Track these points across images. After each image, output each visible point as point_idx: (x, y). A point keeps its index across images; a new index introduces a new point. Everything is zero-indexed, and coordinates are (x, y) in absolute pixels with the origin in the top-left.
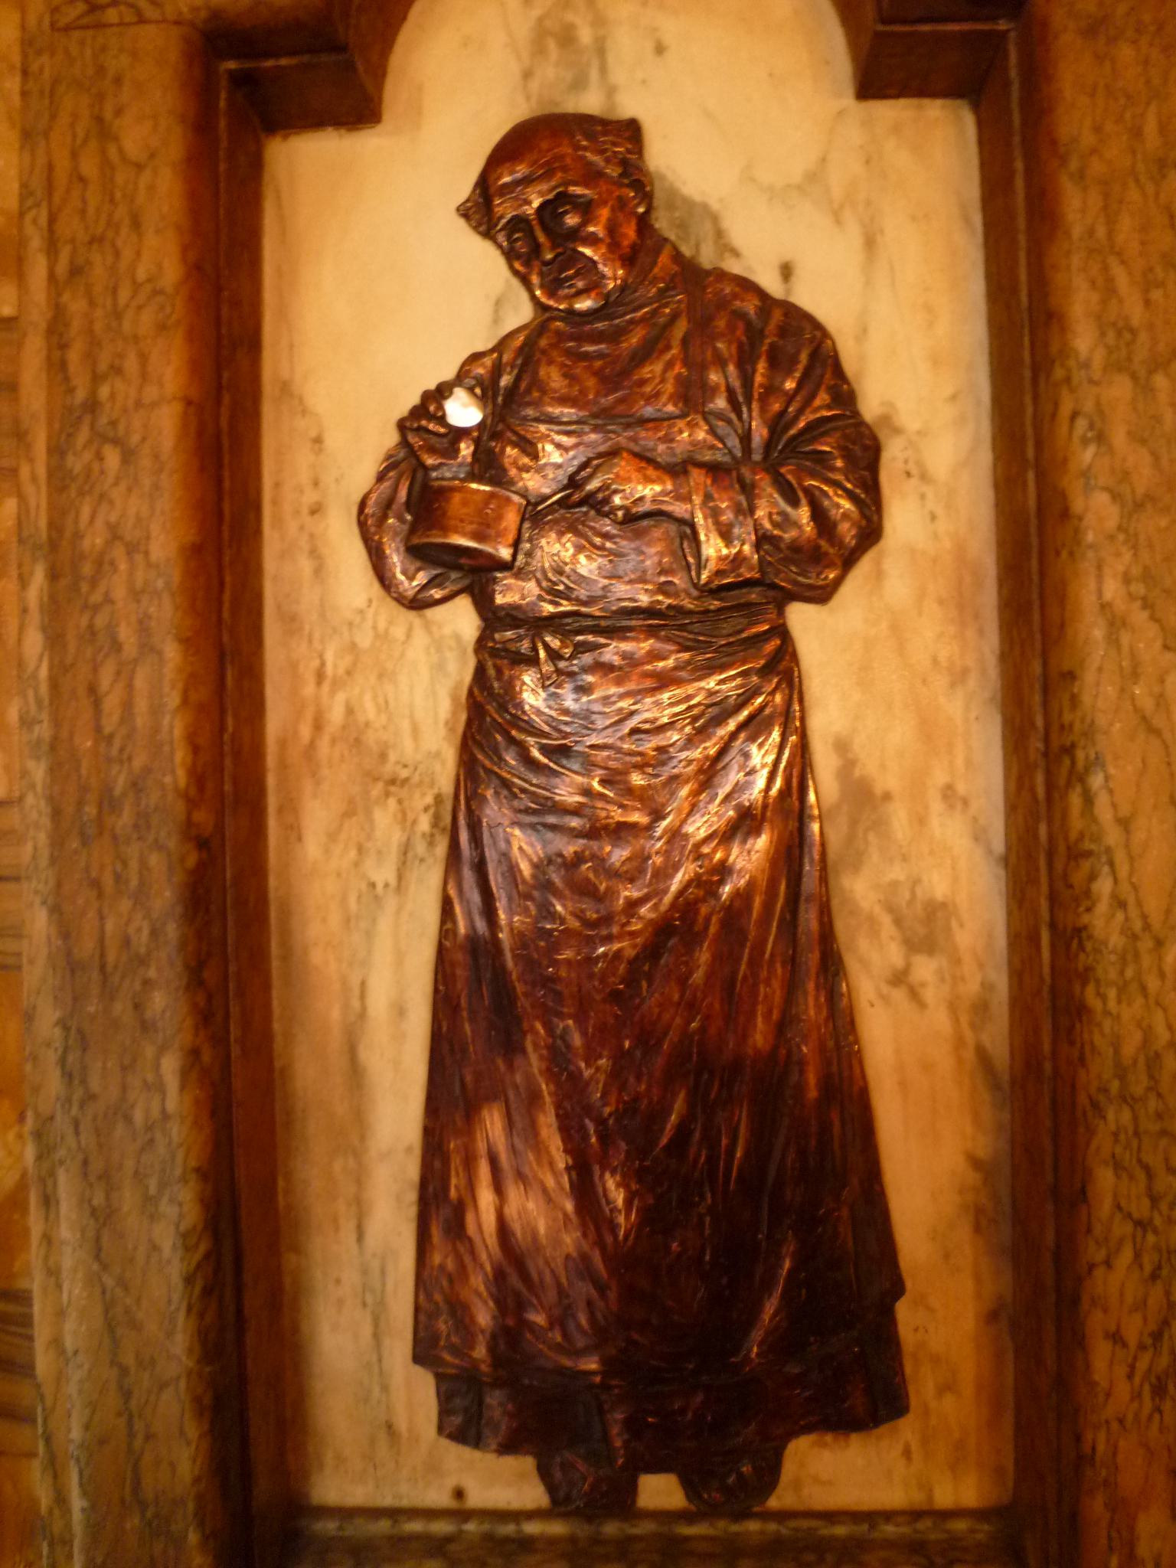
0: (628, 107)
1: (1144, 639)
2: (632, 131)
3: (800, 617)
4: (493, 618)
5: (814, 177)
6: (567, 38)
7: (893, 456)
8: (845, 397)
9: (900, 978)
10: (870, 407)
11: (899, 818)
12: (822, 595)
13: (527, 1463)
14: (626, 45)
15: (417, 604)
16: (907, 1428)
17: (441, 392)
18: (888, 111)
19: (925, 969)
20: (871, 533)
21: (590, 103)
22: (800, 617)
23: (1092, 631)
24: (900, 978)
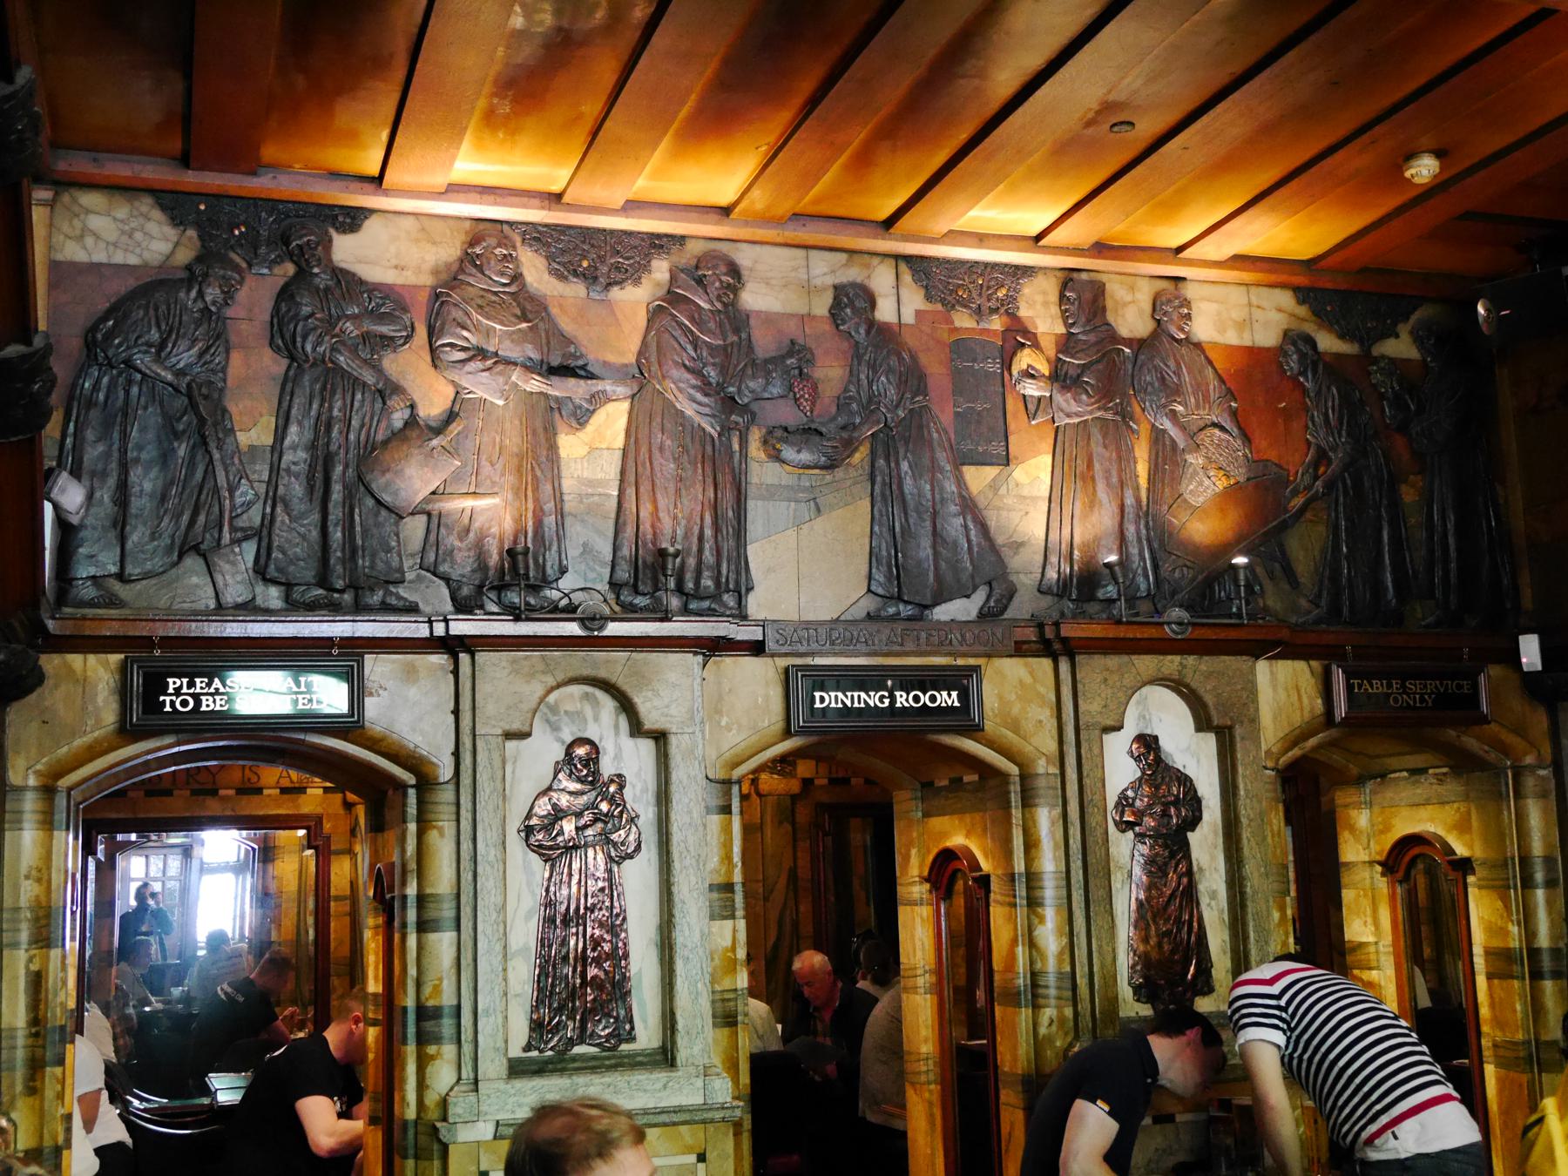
0: (1155, 733)
1: (1253, 843)
2: (1156, 738)
3: (1189, 834)
4: (1137, 835)
5: (1188, 748)
6: (1144, 717)
7: (1204, 803)
8: (1196, 791)
9: (1209, 905)
10: (1200, 794)
11: (1207, 874)
12: (1193, 830)
13: (1149, 1006)
14: (1155, 719)
15: (1123, 831)
16: (1215, 994)
17: (1126, 790)
18: (1201, 735)
19: (1213, 903)
20: (1200, 818)
21: (1148, 731)
22: (1189, 834)
23: (1245, 841)
24: (1209, 905)
